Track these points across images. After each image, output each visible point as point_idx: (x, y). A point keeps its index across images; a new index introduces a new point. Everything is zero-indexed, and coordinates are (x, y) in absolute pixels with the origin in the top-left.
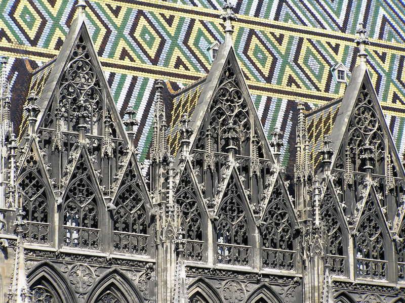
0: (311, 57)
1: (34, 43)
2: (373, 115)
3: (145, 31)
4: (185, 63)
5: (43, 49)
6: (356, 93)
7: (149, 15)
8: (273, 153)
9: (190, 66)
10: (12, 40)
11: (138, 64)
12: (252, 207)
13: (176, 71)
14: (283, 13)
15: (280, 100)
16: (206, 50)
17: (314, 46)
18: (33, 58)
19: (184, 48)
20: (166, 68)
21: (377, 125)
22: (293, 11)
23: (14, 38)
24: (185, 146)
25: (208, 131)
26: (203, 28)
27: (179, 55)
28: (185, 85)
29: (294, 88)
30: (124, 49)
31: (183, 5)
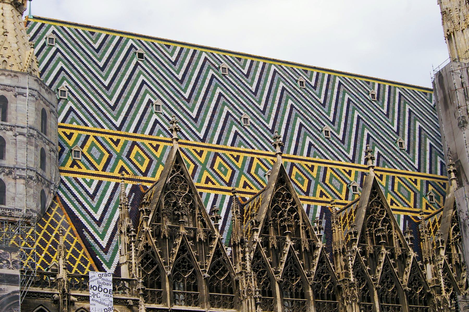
1: (145, 174)
2: (382, 207)
6: (369, 192)
7: (222, 156)
8: (316, 234)
9: (253, 187)
11: (218, 186)
12: (305, 272)
14: (312, 152)
15: (316, 207)
17: (335, 172)
18: (145, 184)
19: (248, 176)
21: (385, 213)
22: (318, 150)
25: (270, 221)
26: (260, 163)
30: (207, 177)
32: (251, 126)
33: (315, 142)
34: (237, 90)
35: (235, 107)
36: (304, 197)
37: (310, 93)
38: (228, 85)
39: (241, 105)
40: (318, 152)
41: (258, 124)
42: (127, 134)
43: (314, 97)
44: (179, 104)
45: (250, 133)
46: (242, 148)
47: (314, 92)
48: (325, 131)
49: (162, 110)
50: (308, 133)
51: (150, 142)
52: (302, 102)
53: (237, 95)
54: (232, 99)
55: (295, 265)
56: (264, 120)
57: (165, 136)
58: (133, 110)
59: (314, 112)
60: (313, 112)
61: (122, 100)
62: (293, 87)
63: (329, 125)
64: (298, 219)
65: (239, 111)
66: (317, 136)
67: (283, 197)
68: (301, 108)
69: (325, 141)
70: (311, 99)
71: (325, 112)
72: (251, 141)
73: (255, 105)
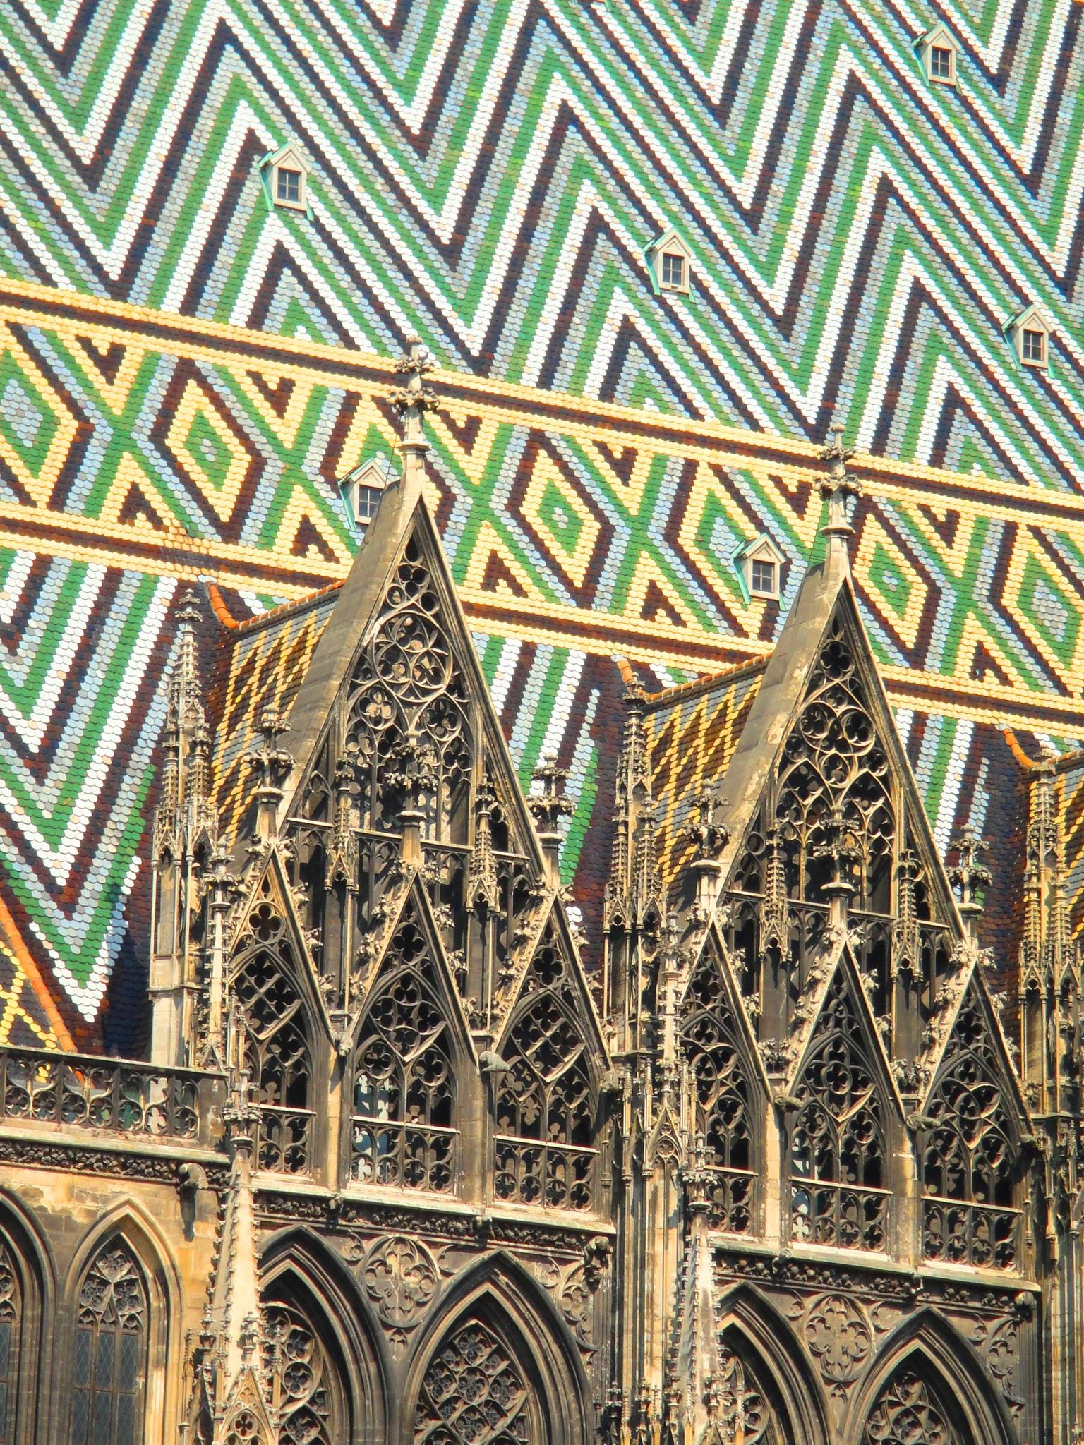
0: (1040, 588)
1: (231, 531)
3: (552, 499)
4: (671, 601)
5: (258, 552)
7: (562, 448)
8: (957, 906)
10: (166, 522)
11: (535, 603)
12: (895, 1070)
13: (646, 628)
14: (955, 442)
15: (950, 724)
16: (731, 562)
18: (230, 580)
19: (669, 554)
20: (617, 618)
23: (172, 515)
24: (705, 881)
25: (771, 835)
27: (654, 577)
28: (676, 673)
29: (990, 686)
31: (661, 416)
32: (695, 296)
33: (974, 388)
34: (640, 92)
35: (625, 188)
36: (899, 671)
37: (975, 115)
38: (603, 60)
39: (655, 178)
40: (981, 444)
41: (726, 286)
42: (153, 316)
43: (990, 136)
44: (378, 164)
45: (686, 334)
46: (648, 414)
47: (992, 109)
48: (1027, 333)
49: (308, 198)
50: (947, 338)
51: (256, 364)
52: (931, 165)
53: (637, 122)
54: (617, 142)
55: (857, 1035)
56: (754, 260)
57: (317, 337)
58: (179, 189)
59: (986, 219)
60: (976, 223)
61: (130, 128)
62: (897, 75)
63: (1047, 297)
64: (888, 829)
65: (643, 211)
66: (987, 357)
67: (834, 733)
68: (923, 199)
69: (1019, 383)
70: (975, 145)
71: (1036, 224)
72: (691, 373)
73: (715, 177)
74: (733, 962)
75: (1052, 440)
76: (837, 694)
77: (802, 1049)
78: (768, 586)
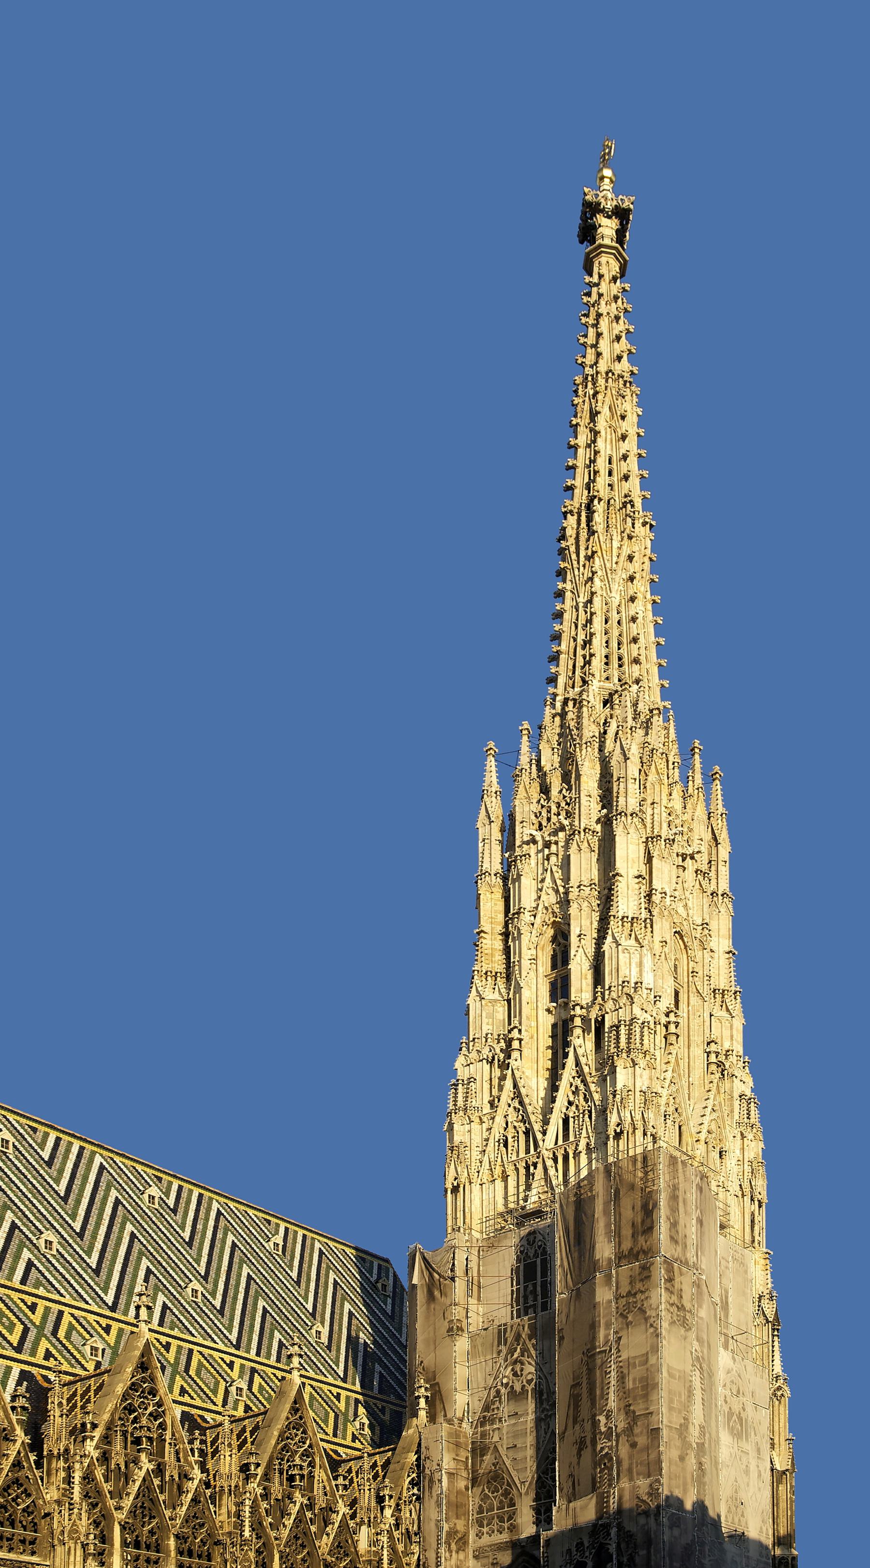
12: (168, 1513)
24: (88, 1440)
74: (99, 1473)
75: (204, 1325)
76: (144, 1380)
77: (129, 1503)
78: (96, 1356)
